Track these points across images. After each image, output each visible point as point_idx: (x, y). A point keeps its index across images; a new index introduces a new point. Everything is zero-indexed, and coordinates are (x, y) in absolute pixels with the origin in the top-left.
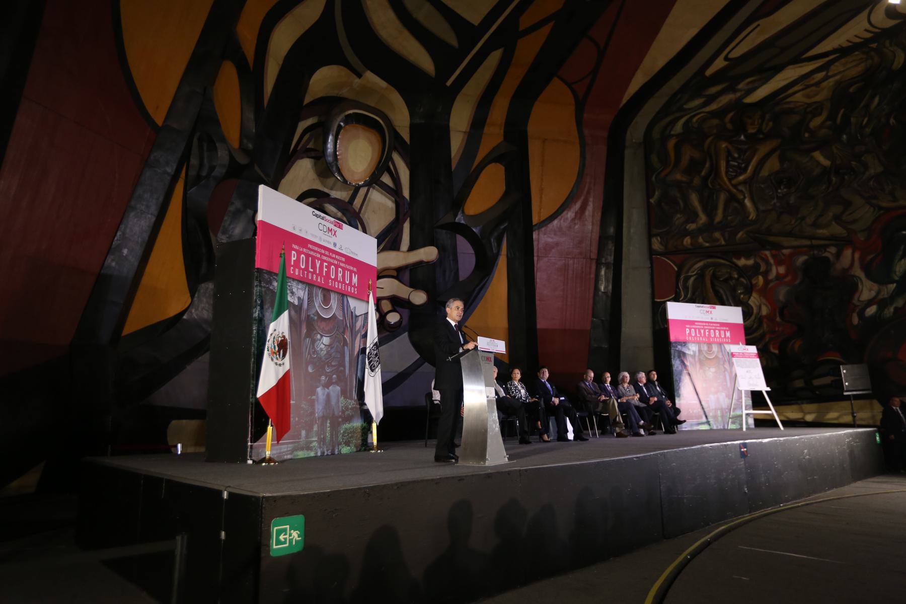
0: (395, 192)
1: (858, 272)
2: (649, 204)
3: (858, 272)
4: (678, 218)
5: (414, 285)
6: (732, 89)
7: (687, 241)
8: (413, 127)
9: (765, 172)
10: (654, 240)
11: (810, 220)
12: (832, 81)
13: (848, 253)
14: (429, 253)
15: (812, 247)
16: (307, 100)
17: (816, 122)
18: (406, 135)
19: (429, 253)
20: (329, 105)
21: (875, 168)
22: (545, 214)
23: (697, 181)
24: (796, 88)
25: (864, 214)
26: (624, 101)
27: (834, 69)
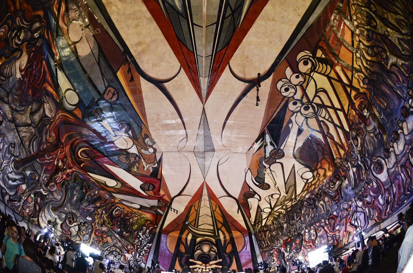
0: (215, 252)
1: (284, 251)
2: (258, 244)
3: (284, 251)
4: (262, 246)
5: (220, 265)
6: (259, 225)
7: (264, 249)
8: (216, 241)
9: (269, 237)
10: (261, 250)
11: (276, 244)
12: (270, 221)
13: (282, 248)
14: (221, 260)
15: (278, 248)
16: (197, 243)
17: (272, 227)
18: (215, 243)
19: (221, 260)
20: (200, 242)
21: (280, 234)
22: (240, 251)
23: (262, 239)
24: (267, 222)
25: (282, 241)
26: (246, 229)
27: (269, 219)
